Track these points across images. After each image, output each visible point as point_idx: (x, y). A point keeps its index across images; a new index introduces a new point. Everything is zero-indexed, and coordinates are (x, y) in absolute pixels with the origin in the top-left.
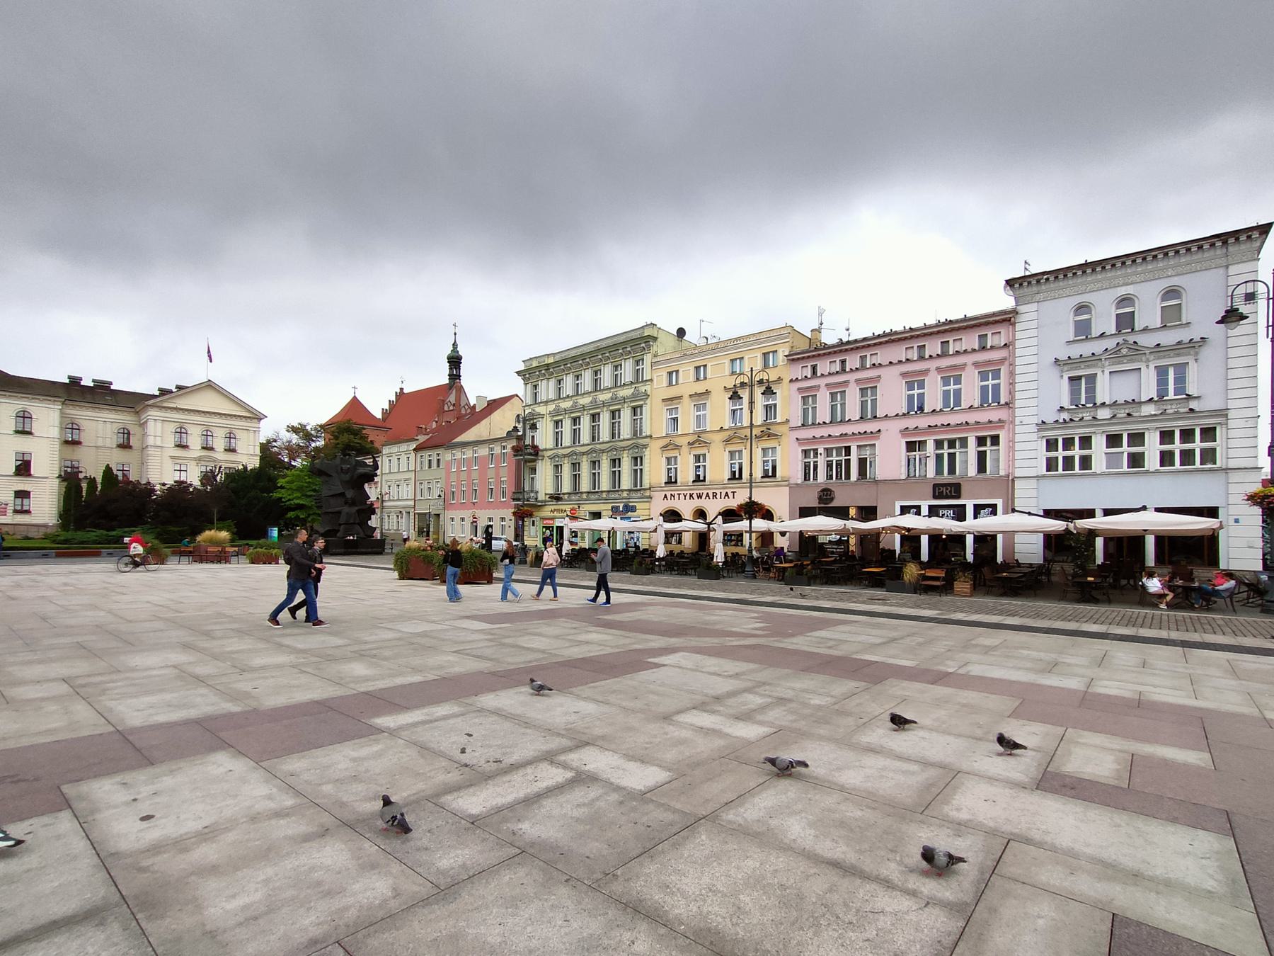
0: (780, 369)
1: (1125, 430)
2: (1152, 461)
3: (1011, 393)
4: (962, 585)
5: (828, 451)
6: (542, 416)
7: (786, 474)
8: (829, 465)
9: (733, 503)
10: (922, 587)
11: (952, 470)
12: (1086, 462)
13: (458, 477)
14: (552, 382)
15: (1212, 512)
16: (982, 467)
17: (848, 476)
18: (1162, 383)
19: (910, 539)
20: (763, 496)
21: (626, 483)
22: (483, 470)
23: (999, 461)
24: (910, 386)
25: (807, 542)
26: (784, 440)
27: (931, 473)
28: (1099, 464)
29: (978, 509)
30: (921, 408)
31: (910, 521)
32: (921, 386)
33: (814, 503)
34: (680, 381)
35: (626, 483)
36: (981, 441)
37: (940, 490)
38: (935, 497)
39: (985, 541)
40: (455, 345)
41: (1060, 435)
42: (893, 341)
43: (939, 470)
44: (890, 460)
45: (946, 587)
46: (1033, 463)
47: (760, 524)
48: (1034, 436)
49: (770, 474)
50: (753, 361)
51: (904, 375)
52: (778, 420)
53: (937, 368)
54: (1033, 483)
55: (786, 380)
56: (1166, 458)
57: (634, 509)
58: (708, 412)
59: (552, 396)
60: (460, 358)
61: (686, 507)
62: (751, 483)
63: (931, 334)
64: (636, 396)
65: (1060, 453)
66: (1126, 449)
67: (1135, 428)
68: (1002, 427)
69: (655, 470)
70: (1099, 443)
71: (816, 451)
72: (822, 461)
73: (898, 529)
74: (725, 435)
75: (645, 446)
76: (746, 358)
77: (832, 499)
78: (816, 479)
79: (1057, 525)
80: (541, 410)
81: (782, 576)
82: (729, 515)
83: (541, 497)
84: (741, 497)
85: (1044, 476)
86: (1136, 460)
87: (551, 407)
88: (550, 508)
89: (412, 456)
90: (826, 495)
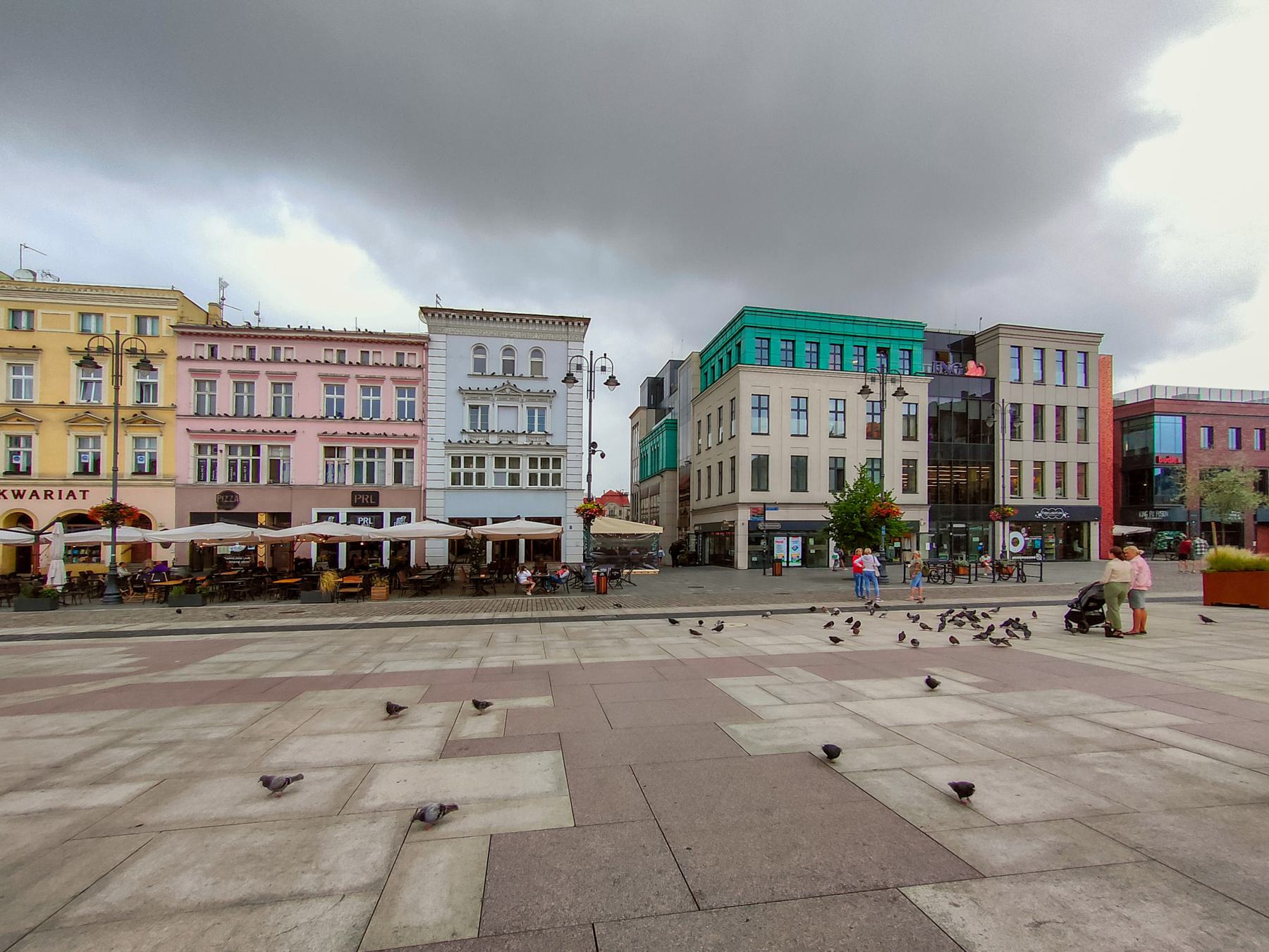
0: (161, 338)
1: (507, 454)
2: (524, 482)
3: (424, 411)
4: (379, 589)
8: (232, 465)
9: (83, 506)
10: (341, 595)
11: (371, 479)
12: (481, 478)
15: (557, 521)
16: (398, 479)
18: (531, 420)
19: (328, 547)
20: (131, 497)
23: (415, 474)
24: (329, 389)
25: (201, 555)
26: (168, 429)
27: (350, 481)
28: (490, 481)
29: (394, 516)
30: (340, 415)
31: (327, 528)
33: (213, 508)
36: (398, 453)
37: (359, 498)
38: (354, 505)
39: (400, 547)
41: (462, 453)
42: (311, 339)
43: (358, 479)
44: (306, 465)
45: (365, 592)
46: (440, 476)
47: (128, 533)
48: (442, 453)
49: (147, 470)
50: (118, 323)
51: (323, 377)
52: (160, 403)
53: (357, 376)
54: (441, 495)
55: (172, 357)
56: (533, 478)
58: (36, 377)
62: (115, 479)
63: (352, 341)
65: (462, 470)
66: (507, 470)
67: (515, 453)
70: (490, 462)
71: (215, 449)
72: (222, 460)
73: (315, 536)
74: (71, 414)
77: (236, 504)
78: (214, 479)
79: (459, 532)
81: (164, 597)
82: (75, 521)
84: (98, 497)
85: (449, 489)
86: (514, 479)
90: (228, 498)
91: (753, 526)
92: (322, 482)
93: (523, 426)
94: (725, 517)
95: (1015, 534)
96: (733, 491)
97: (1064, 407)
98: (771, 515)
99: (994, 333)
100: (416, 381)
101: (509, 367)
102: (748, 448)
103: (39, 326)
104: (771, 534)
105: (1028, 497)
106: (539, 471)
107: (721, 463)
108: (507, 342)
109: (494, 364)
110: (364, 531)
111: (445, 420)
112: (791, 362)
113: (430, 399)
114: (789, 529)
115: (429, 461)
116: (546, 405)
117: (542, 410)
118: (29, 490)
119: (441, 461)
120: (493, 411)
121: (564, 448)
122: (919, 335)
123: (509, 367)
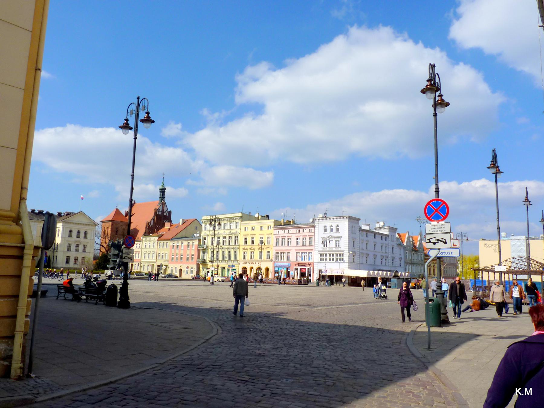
6: (208, 235)
13: (175, 252)
21: (232, 259)
22: (185, 251)
35: (232, 259)
40: (163, 183)
43: (302, 260)
49: (268, 257)
57: (234, 266)
60: (165, 189)
61: (248, 267)
65: (322, 257)
69: (240, 256)
70: (328, 255)
80: (208, 233)
89: (156, 242)
101: (331, 230)
106: (339, 257)
121: (343, 251)
123: (331, 230)
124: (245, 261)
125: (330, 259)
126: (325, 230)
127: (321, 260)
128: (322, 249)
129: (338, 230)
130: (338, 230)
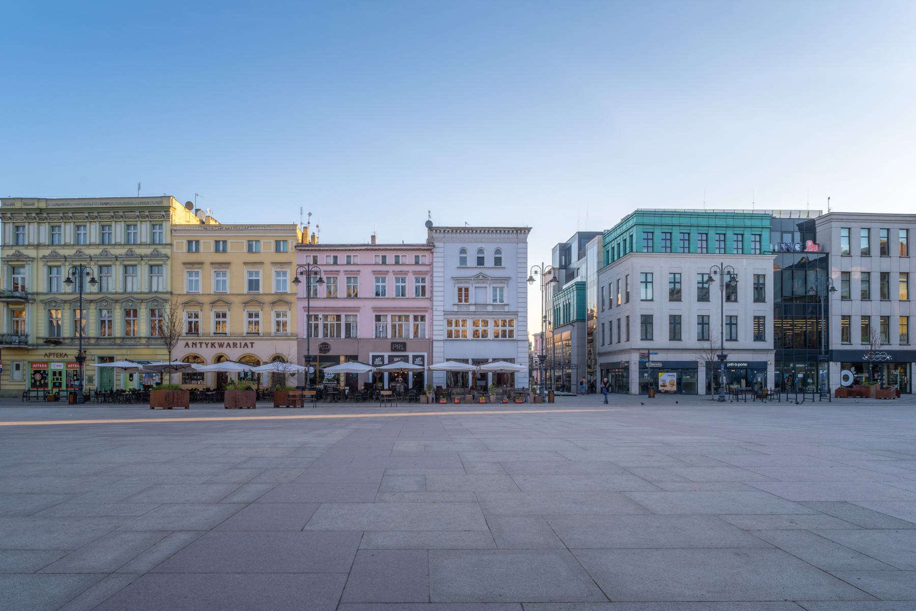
3: (432, 292)
5: (326, 317)
7: (295, 331)
8: (325, 326)
14: (45, 229)
15: (512, 361)
17: (339, 335)
18: (495, 295)
24: (377, 280)
32: (384, 281)
34: (201, 249)
44: (365, 328)
46: (441, 333)
48: (442, 318)
51: (374, 272)
54: (441, 344)
58: (227, 278)
59: (44, 239)
64: (156, 255)
65: (453, 328)
68: (427, 311)
71: (316, 318)
75: (166, 301)
76: (262, 242)
77: (329, 350)
83: (31, 340)
87: (46, 252)
88: (43, 352)
90: (324, 347)
91: (643, 367)
92: (374, 337)
93: (490, 301)
94: (622, 358)
95: (845, 372)
96: (628, 340)
97: (888, 273)
98: (653, 358)
99: (832, 217)
100: (426, 273)
101: (481, 261)
102: (638, 309)
103: (229, 249)
104: (655, 371)
105: (857, 343)
107: (619, 320)
108: (480, 245)
109: (472, 261)
110: (401, 365)
111: (443, 298)
112: (669, 249)
113: (435, 284)
114: (668, 367)
115: (435, 323)
116: (505, 285)
117: (502, 289)
118: (226, 342)
119: (441, 323)
120: (472, 292)
122: (767, 223)
123: (481, 261)
124: (191, 339)
125: (476, 334)
126: (463, 261)
127: (450, 334)
128: (455, 309)
129: (498, 261)
130: (498, 261)
